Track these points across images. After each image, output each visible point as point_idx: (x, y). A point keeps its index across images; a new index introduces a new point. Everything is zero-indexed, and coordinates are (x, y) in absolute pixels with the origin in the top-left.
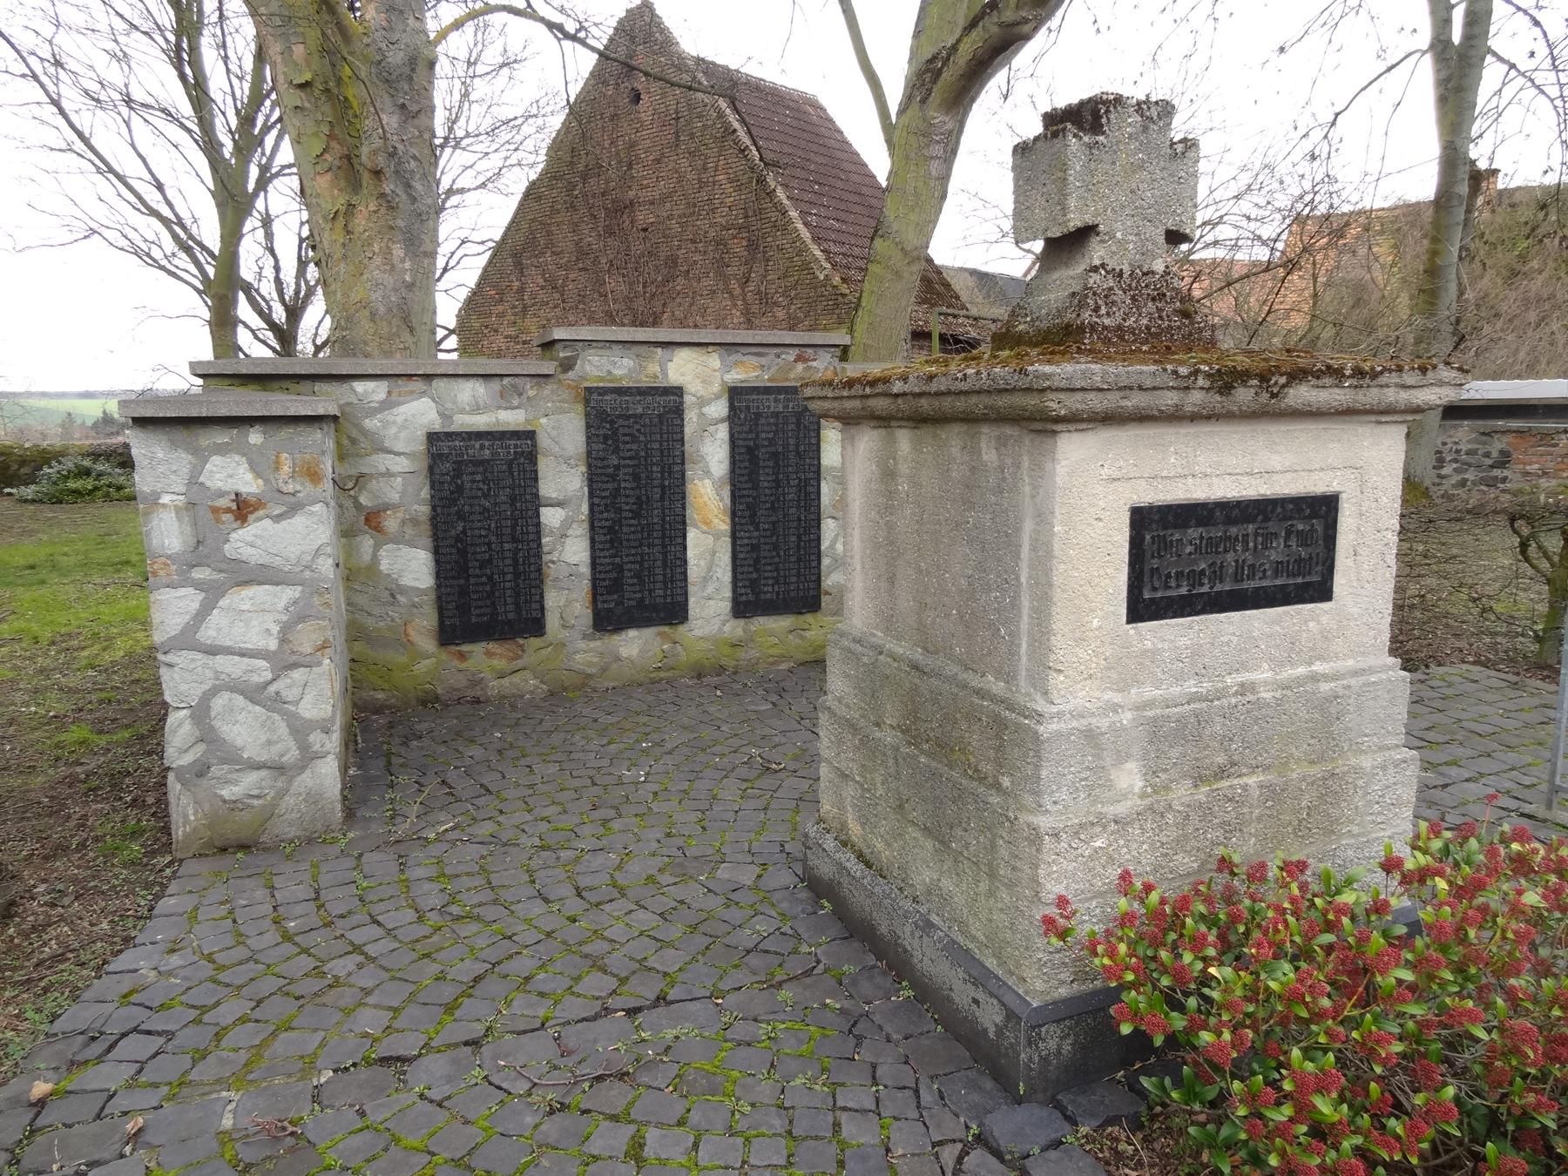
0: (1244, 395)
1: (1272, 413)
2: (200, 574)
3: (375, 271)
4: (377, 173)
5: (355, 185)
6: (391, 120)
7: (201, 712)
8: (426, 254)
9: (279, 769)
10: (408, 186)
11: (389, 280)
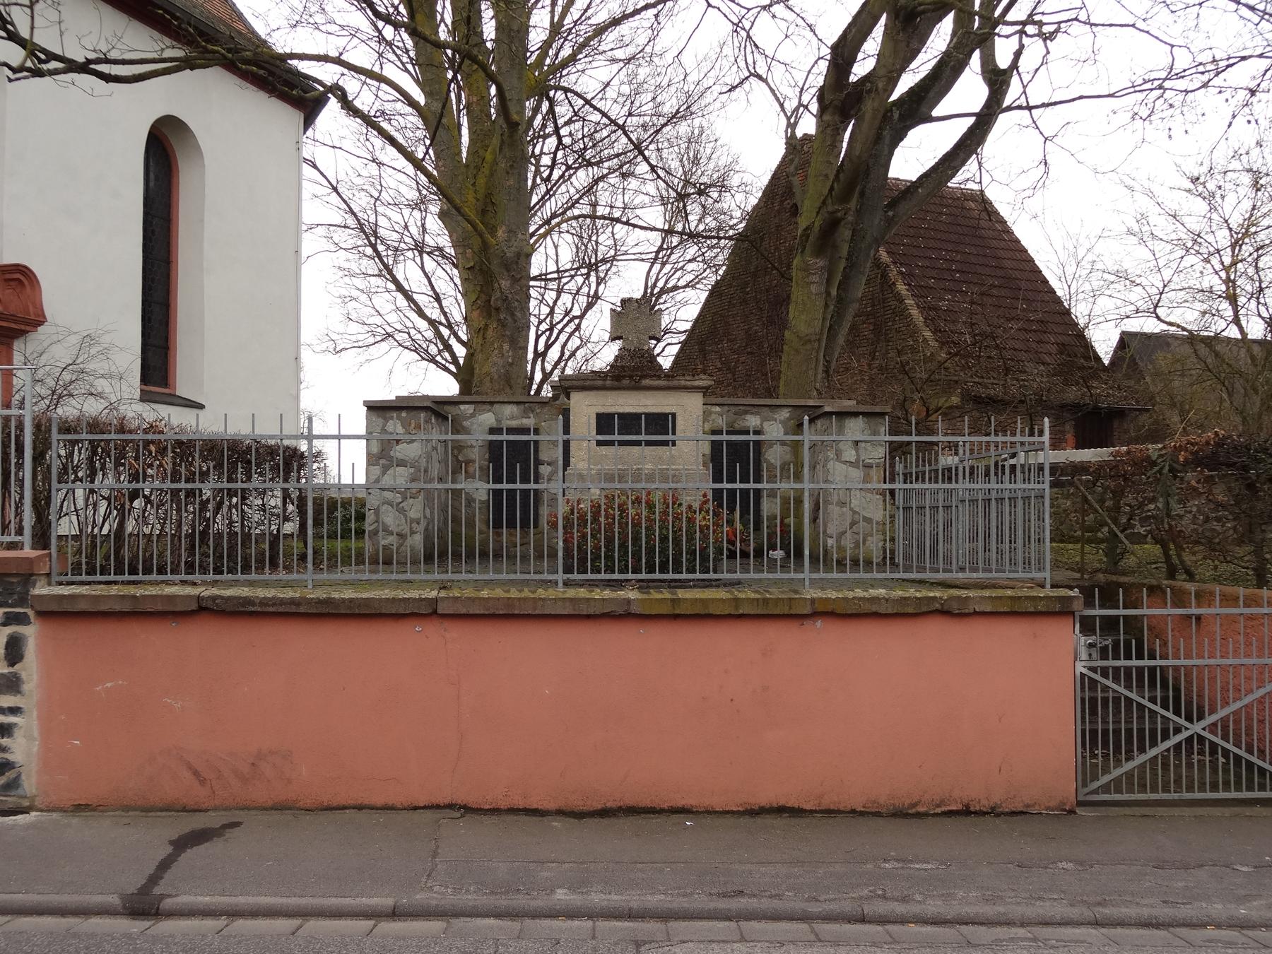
0: (626, 382)
1: (637, 388)
2: (382, 461)
3: (495, 358)
4: (497, 309)
5: (489, 316)
6: (505, 284)
7: (377, 511)
8: (520, 348)
9: (400, 535)
10: (513, 315)
11: (501, 362)
